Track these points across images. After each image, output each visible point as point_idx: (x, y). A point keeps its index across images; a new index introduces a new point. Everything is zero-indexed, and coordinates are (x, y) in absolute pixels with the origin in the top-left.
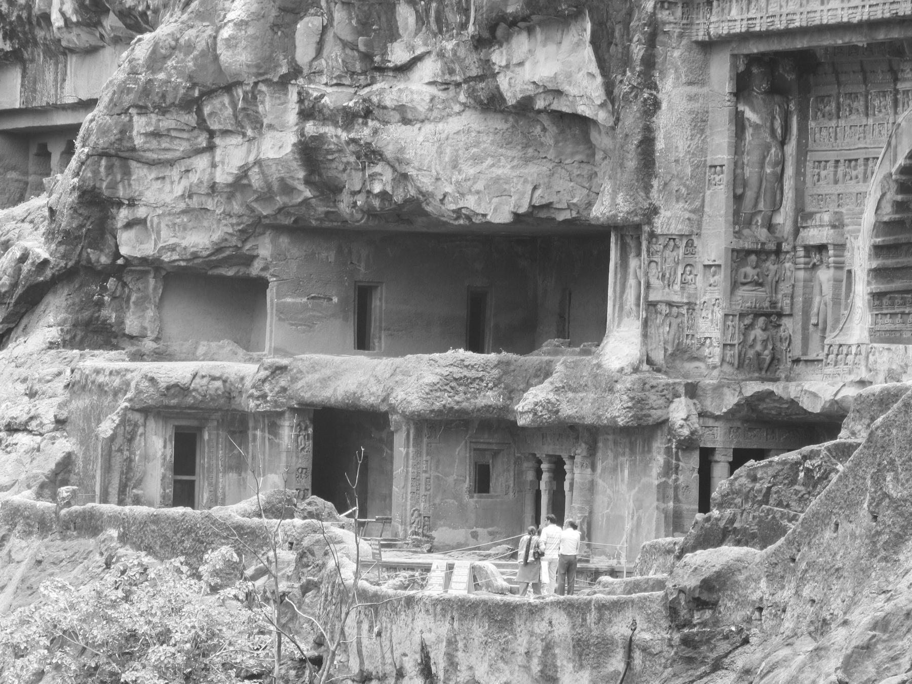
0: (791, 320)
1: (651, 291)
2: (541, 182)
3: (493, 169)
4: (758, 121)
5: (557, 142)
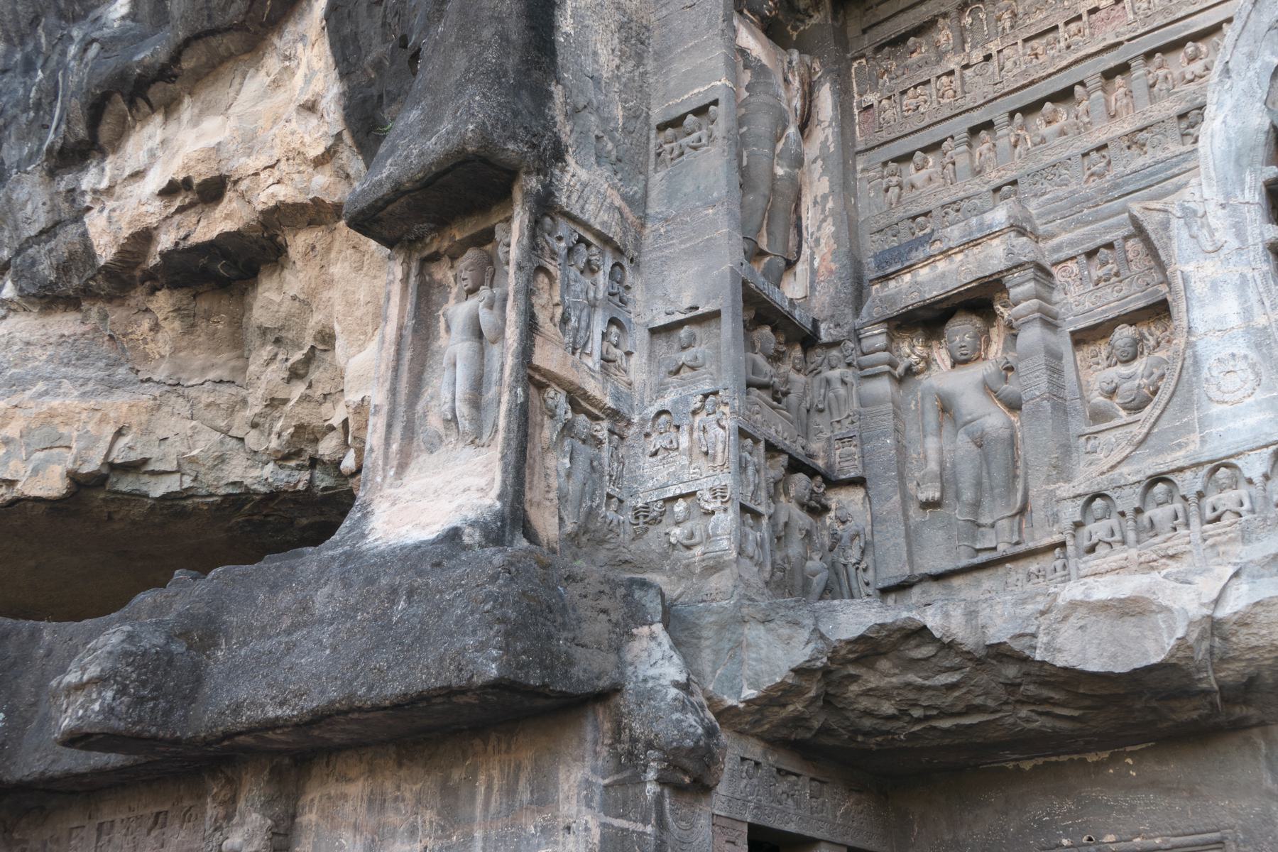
0: (858, 494)
1: (539, 340)
2: (135, 420)
3: (46, 399)
4: (765, 61)
5: (175, 350)
